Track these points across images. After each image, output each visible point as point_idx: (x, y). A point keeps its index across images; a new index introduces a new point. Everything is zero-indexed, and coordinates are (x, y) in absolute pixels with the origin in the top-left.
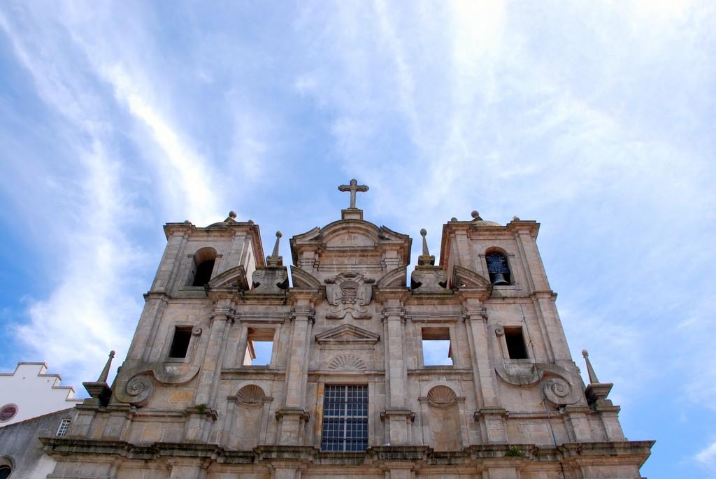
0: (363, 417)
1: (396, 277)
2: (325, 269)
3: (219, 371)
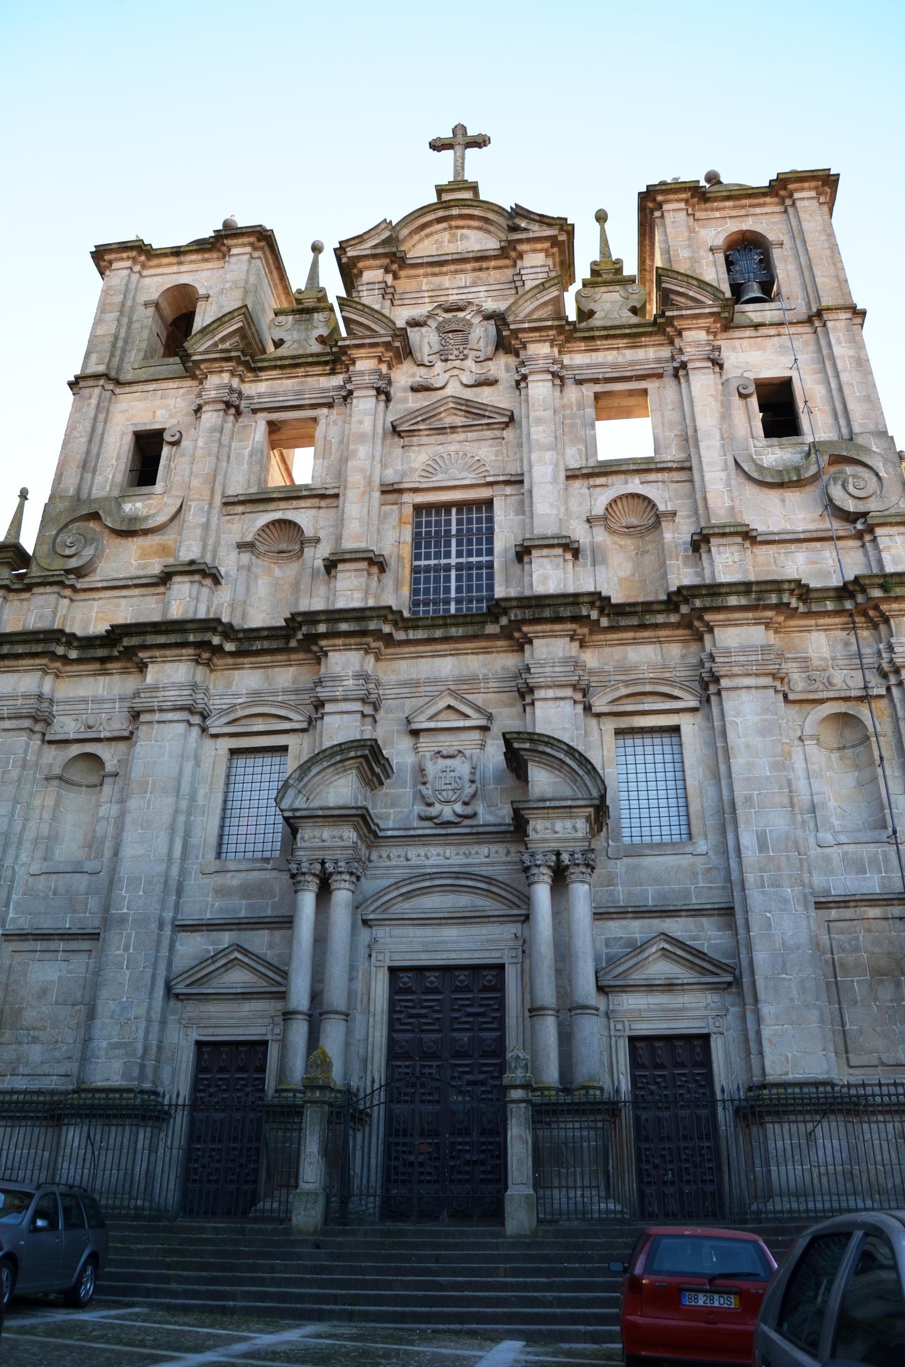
0: (484, 559)
1: (542, 300)
2: (407, 302)
3: (218, 501)
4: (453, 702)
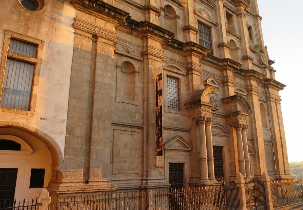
4: (214, 80)
